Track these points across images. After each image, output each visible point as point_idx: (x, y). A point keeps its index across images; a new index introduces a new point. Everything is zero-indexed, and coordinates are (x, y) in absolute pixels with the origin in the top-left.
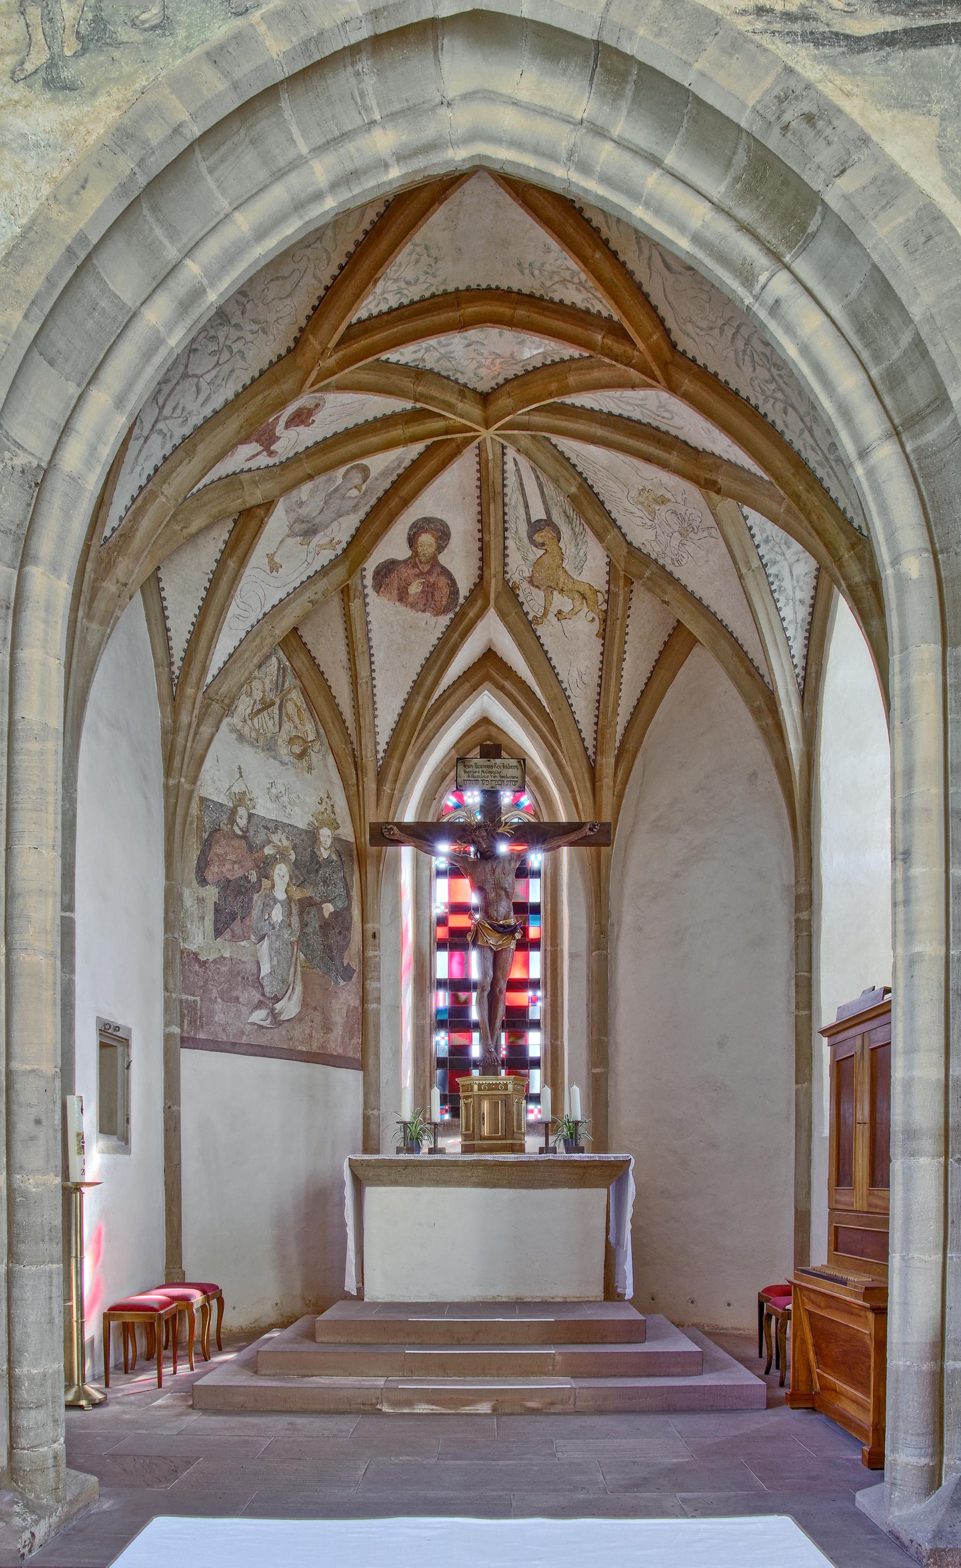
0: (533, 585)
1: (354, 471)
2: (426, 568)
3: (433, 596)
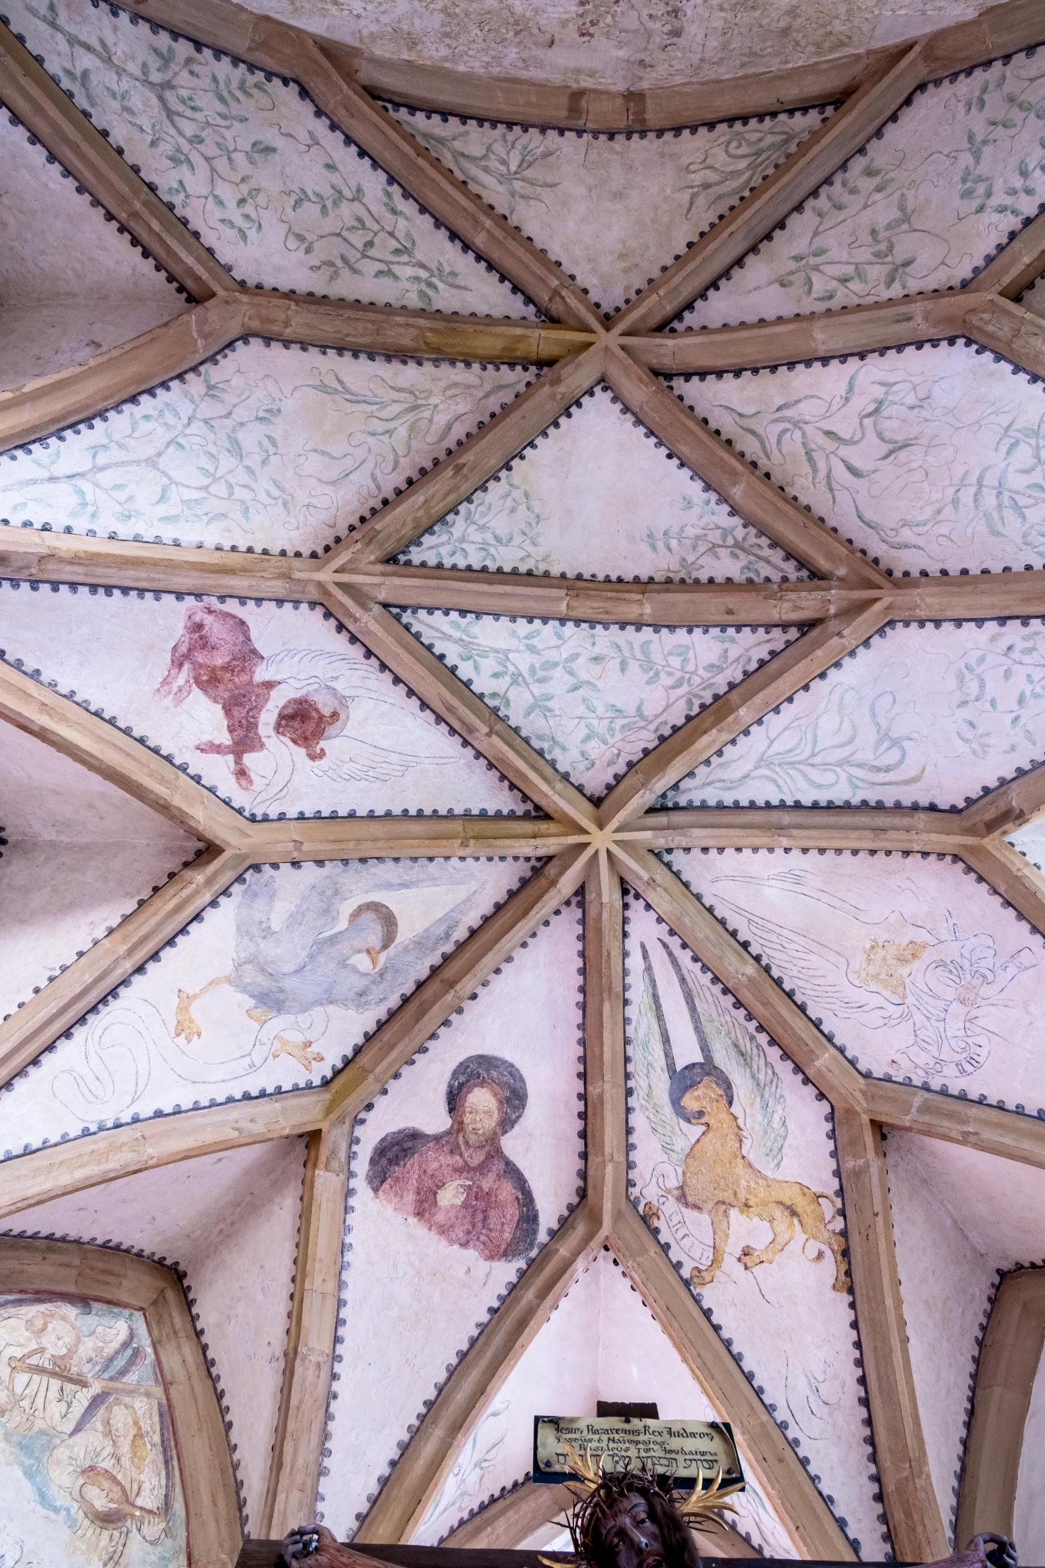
0: (687, 1205)
1: (369, 916)
2: (477, 1158)
3: (485, 1218)
